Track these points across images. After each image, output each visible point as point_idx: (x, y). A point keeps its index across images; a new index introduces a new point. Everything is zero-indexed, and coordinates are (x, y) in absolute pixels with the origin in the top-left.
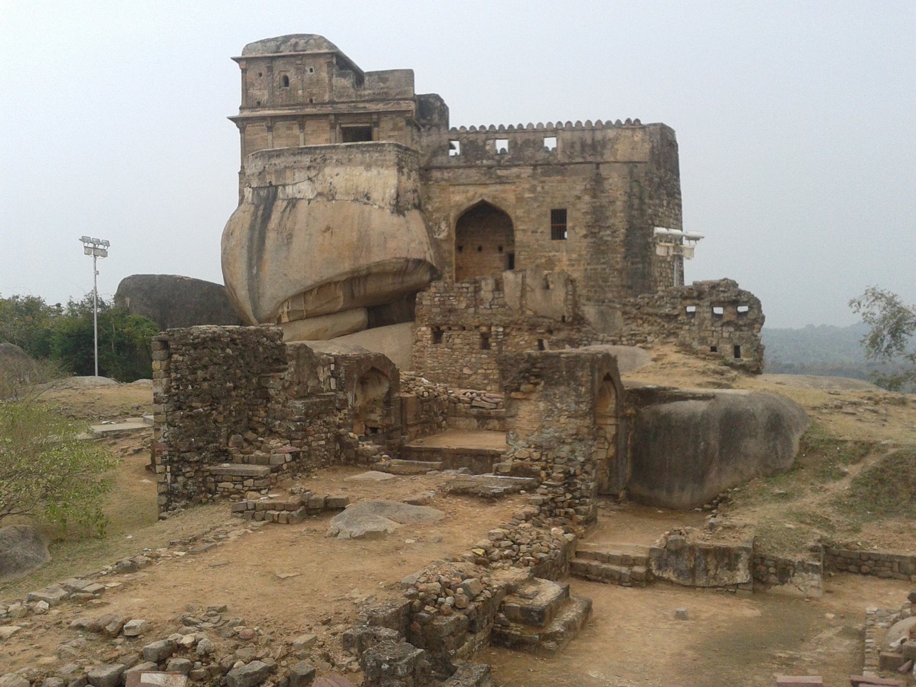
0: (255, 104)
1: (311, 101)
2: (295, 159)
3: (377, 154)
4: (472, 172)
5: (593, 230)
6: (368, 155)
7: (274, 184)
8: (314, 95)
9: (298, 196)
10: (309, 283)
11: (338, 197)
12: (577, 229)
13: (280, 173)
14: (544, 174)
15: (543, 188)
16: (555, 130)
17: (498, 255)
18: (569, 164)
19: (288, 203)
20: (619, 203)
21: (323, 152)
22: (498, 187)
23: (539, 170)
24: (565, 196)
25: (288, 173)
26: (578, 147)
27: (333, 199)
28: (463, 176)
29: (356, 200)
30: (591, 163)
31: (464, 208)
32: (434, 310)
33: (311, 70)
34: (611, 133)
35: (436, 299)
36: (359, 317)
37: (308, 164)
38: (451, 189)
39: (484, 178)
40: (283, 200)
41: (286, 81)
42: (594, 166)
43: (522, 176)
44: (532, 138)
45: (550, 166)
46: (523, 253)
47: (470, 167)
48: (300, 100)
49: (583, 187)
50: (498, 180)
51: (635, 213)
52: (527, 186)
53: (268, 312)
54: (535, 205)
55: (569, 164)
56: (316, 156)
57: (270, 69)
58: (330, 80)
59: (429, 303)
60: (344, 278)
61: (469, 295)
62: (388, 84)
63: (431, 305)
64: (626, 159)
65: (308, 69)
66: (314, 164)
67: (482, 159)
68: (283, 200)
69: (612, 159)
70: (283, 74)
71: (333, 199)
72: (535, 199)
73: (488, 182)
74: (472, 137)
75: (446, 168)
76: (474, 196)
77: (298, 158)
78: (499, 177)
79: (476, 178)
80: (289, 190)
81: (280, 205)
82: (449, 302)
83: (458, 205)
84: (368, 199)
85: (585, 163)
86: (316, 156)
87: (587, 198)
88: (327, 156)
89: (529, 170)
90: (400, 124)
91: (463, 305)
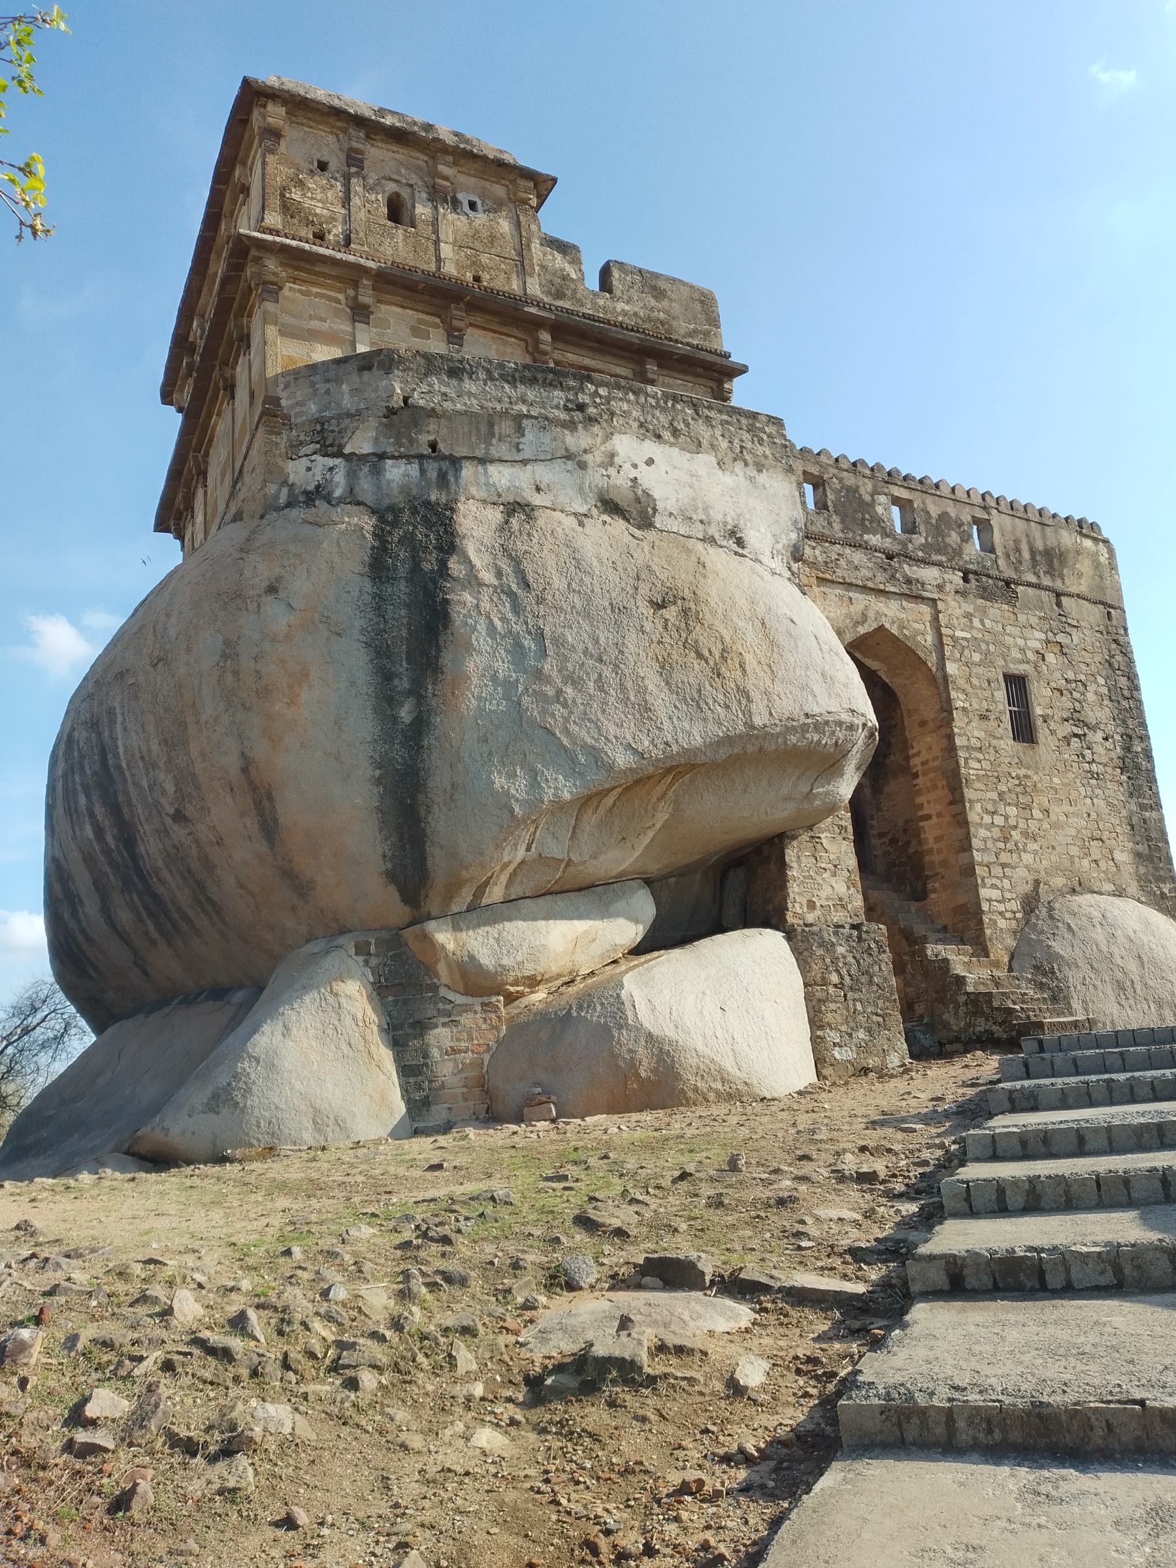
11: (658, 521)
30: (1047, 589)
47: (855, 546)
50: (905, 589)
54: (976, 657)
74: (850, 479)
76: (864, 618)
78: (909, 581)
79: (865, 573)
84: (740, 542)
85: (1037, 586)
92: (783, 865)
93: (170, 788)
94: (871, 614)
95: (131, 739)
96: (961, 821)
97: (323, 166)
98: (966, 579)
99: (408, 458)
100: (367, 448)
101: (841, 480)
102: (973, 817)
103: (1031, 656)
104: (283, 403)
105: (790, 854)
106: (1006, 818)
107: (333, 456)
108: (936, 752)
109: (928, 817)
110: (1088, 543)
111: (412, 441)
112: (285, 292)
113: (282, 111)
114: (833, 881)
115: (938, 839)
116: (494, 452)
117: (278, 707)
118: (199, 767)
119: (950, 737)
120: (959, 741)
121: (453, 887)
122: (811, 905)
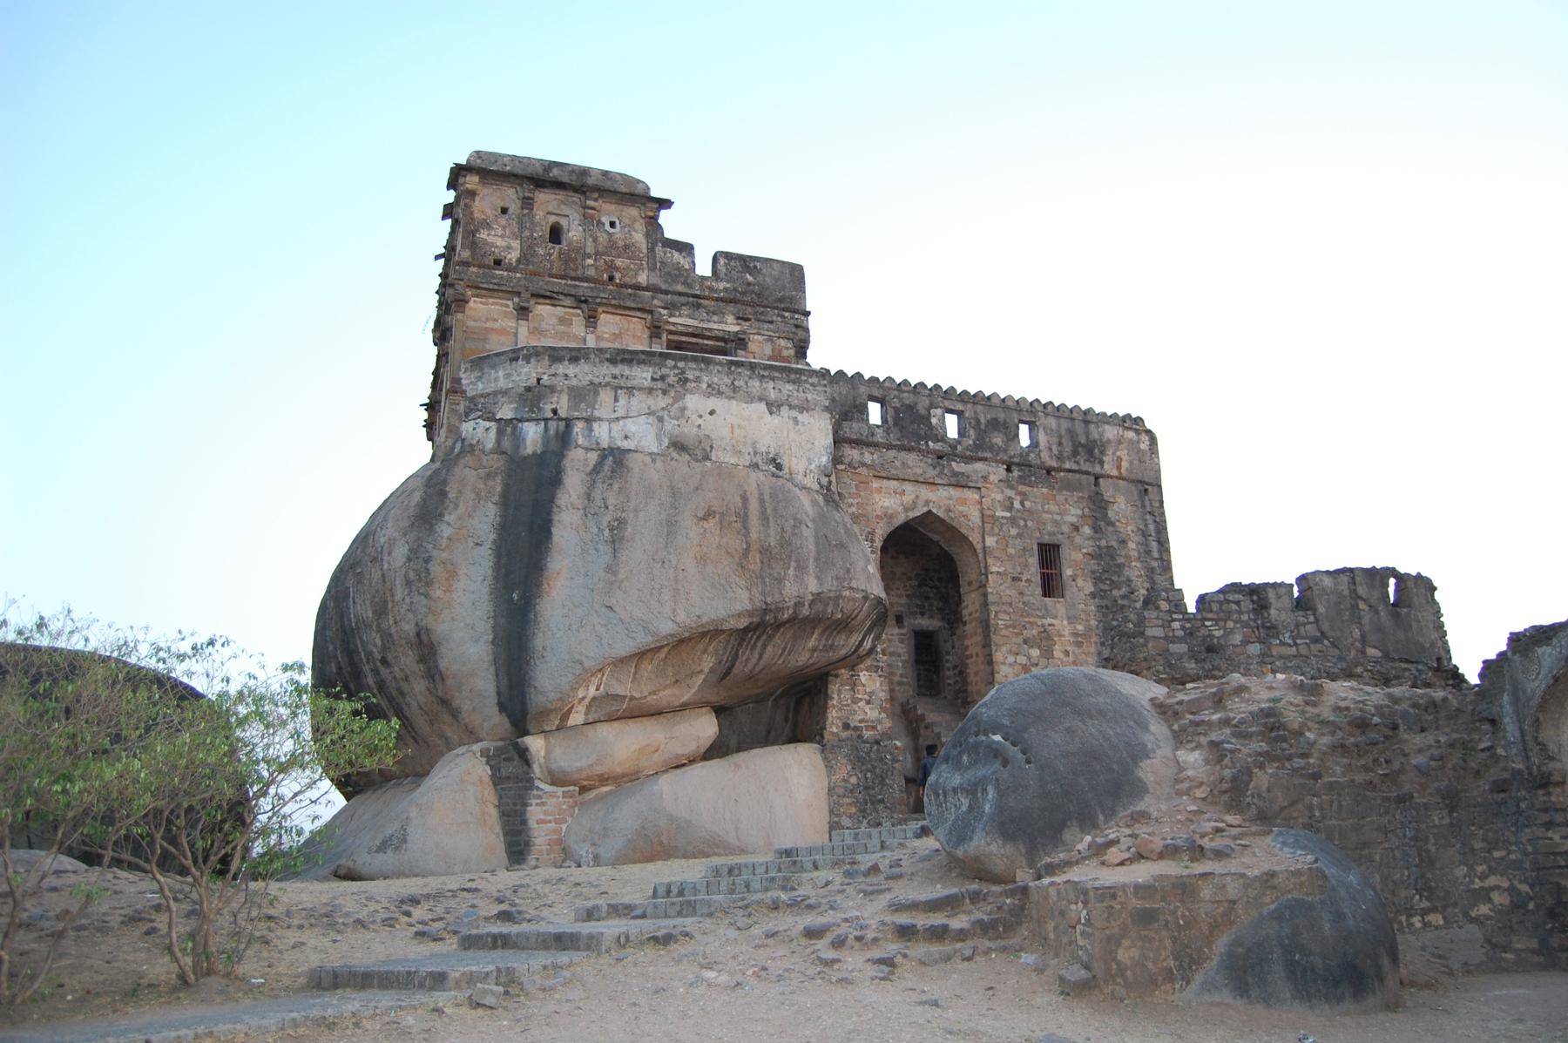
0: (491, 259)
1: (611, 278)
2: (616, 370)
3: (790, 387)
4: (911, 458)
5: (1102, 586)
6: (771, 384)
7: (563, 413)
8: (617, 269)
9: (625, 445)
10: (667, 628)
12: (1080, 582)
13: (581, 395)
14: (1023, 480)
15: (1022, 503)
16: (1032, 412)
17: (897, 631)
18: (1060, 470)
19: (603, 458)
20: (1132, 545)
21: (681, 364)
22: (953, 492)
23: (1016, 473)
24: (1056, 523)
25: (605, 396)
26: (1068, 448)
27: (707, 458)
28: (897, 463)
29: (755, 466)
30: (1087, 473)
31: (901, 519)
32: (1174, 648)
33: (612, 224)
34: (1110, 432)
35: (1176, 625)
36: (705, 728)
37: (646, 384)
38: (875, 484)
39: (931, 473)
40: (587, 449)
41: (556, 234)
42: (1092, 479)
43: (992, 478)
44: (1001, 416)
45: (1023, 468)
46: (1001, 616)
47: (910, 450)
48: (591, 272)
49: (1079, 512)
50: (953, 480)
51: (1155, 564)
52: (999, 497)
53: (553, 696)
54: (1014, 532)
55: (1060, 470)
56: (665, 371)
57: (527, 203)
58: (651, 250)
59: (1159, 632)
60: (743, 623)
61: (1245, 617)
62: (760, 278)
63: (1166, 638)
64: (1134, 477)
65: (606, 220)
66: (660, 384)
67: (927, 438)
68: (587, 449)
69: (1115, 473)
70: (552, 219)
71: (707, 458)
72: (1013, 521)
73: (938, 481)
74: (908, 398)
75: (868, 445)
76: (914, 505)
77: (625, 370)
78: (955, 474)
79: (920, 471)
80: (602, 432)
81: (577, 462)
82: (1204, 632)
83: (888, 516)
84: (779, 467)
86: (665, 371)
87: (1087, 530)
88: (690, 375)
89: (1002, 469)
90: (785, 353)
91: (1237, 639)
92: (827, 697)
93: (379, 643)
94: (920, 503)
95: (361, 609)
96: (990, 662)
97: (504, 211)
98: (1009, 470)
99: (537, 420)
100: (510, 415)
101: (901, 400)
102: (998, 656)
103: (1065, 528)
104: (464, 382)
105: (833, 688)
106: (1029, 658)
107: (488, 419)
108: (977, 606)
109: (971, 656)
110: (1131, 434)
111: (540, 409)
112: (471, 304)
113: (476, 179)
114: (867, 708)
115: (976, 673)
116: (596, 413)
117: (439, 593)
118: (393, 630)
119: (985, 595)
120: (991, 598)
121: (545, 713)
122: (846, 726)
